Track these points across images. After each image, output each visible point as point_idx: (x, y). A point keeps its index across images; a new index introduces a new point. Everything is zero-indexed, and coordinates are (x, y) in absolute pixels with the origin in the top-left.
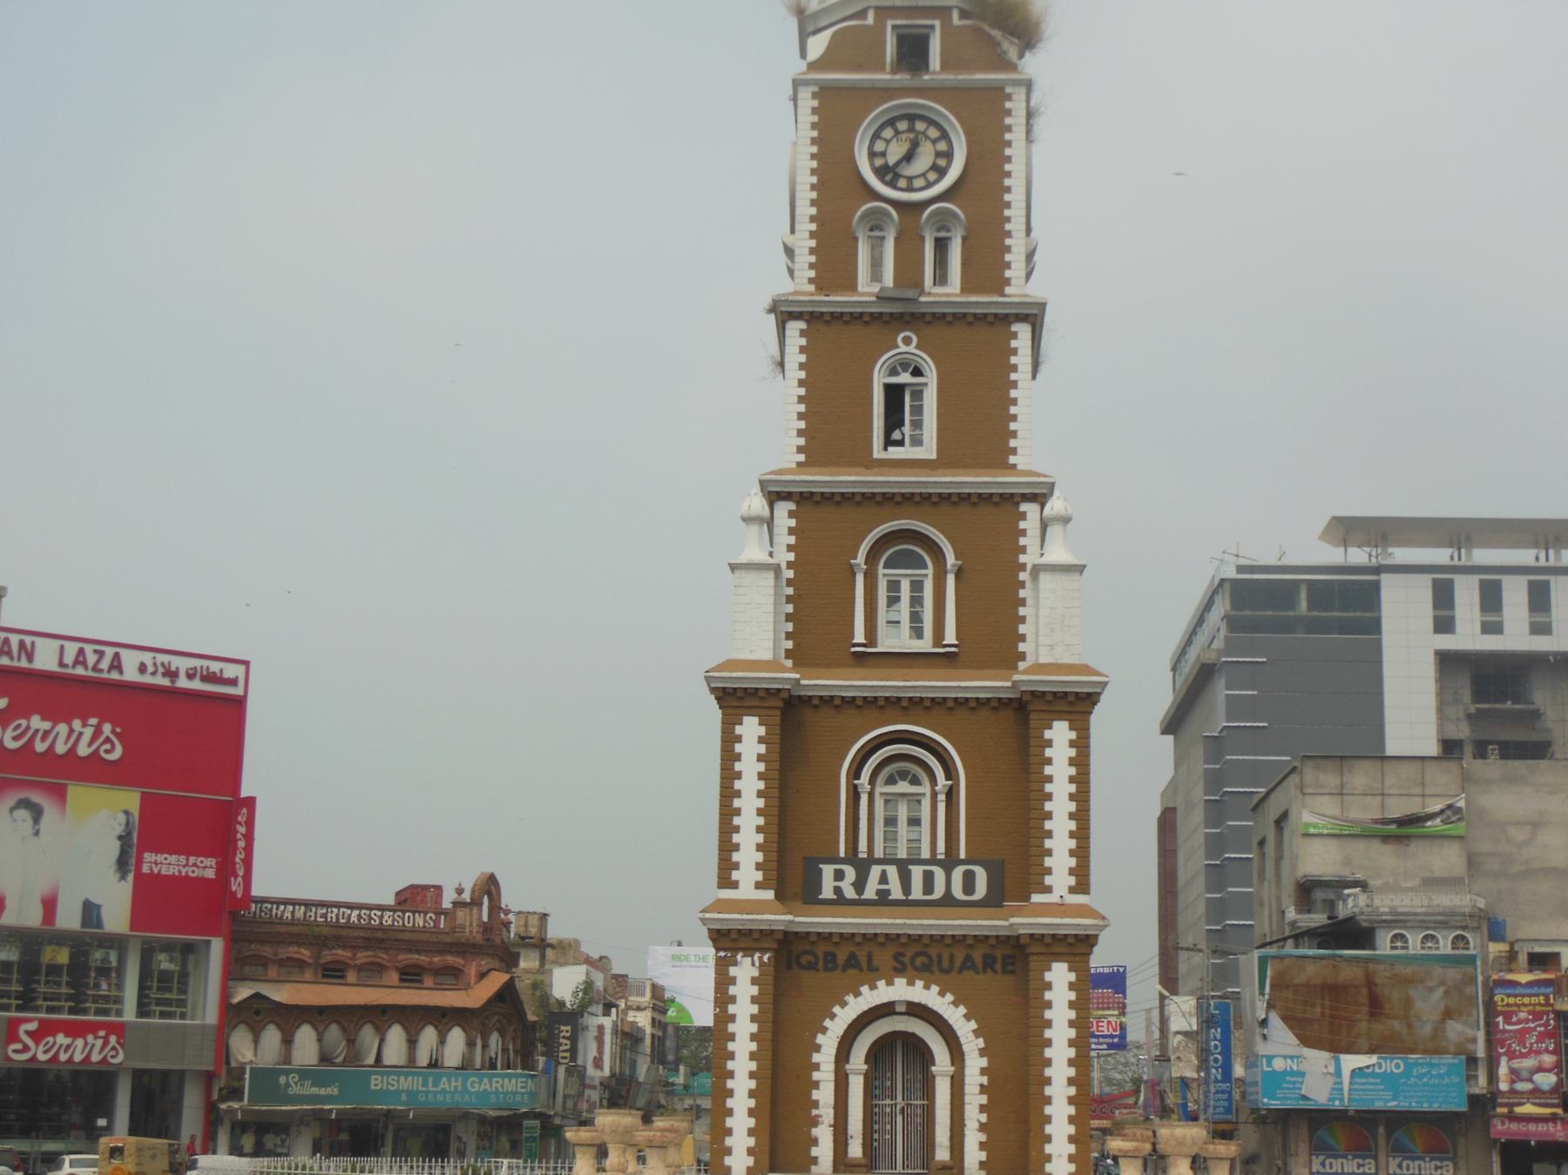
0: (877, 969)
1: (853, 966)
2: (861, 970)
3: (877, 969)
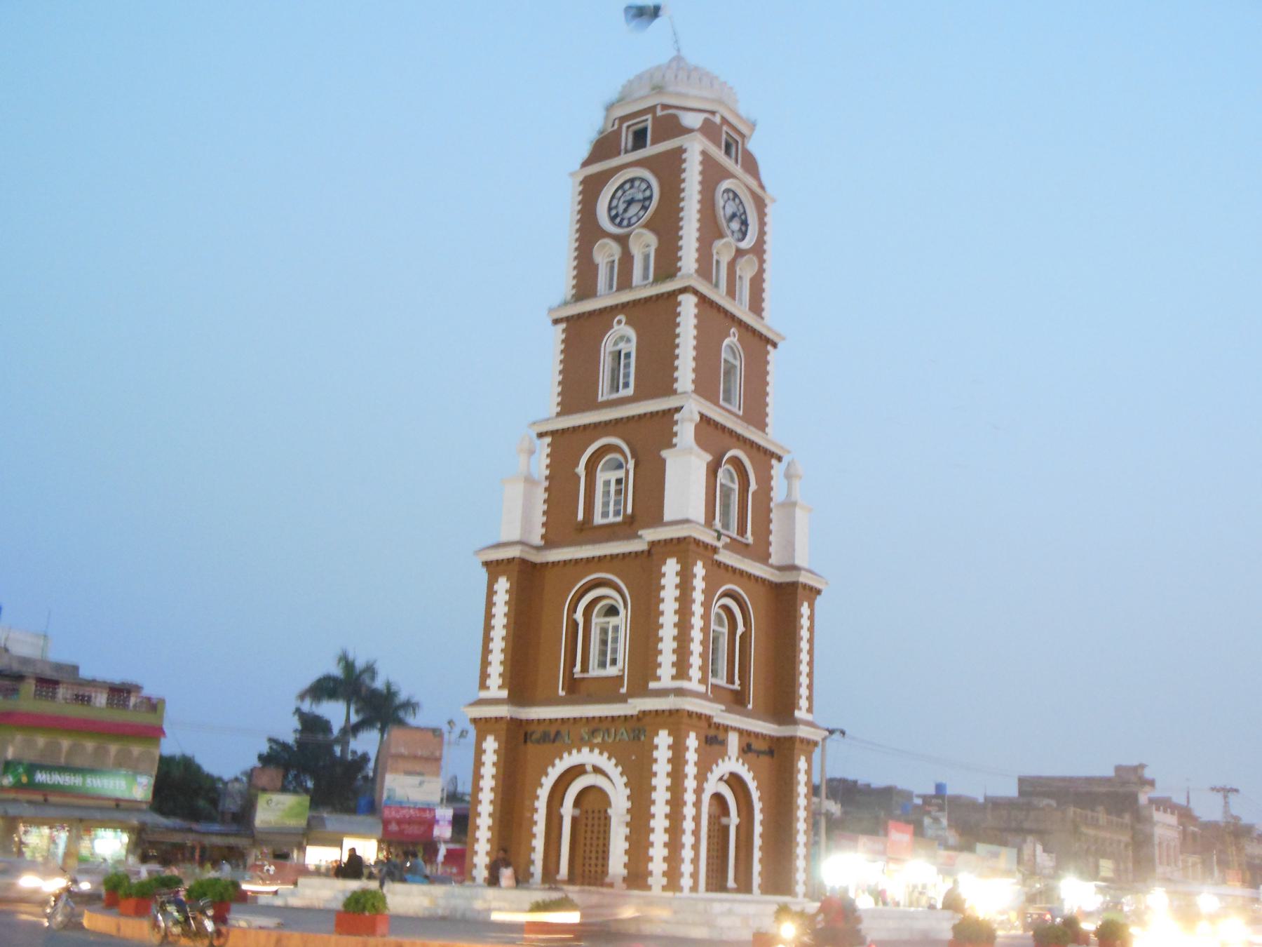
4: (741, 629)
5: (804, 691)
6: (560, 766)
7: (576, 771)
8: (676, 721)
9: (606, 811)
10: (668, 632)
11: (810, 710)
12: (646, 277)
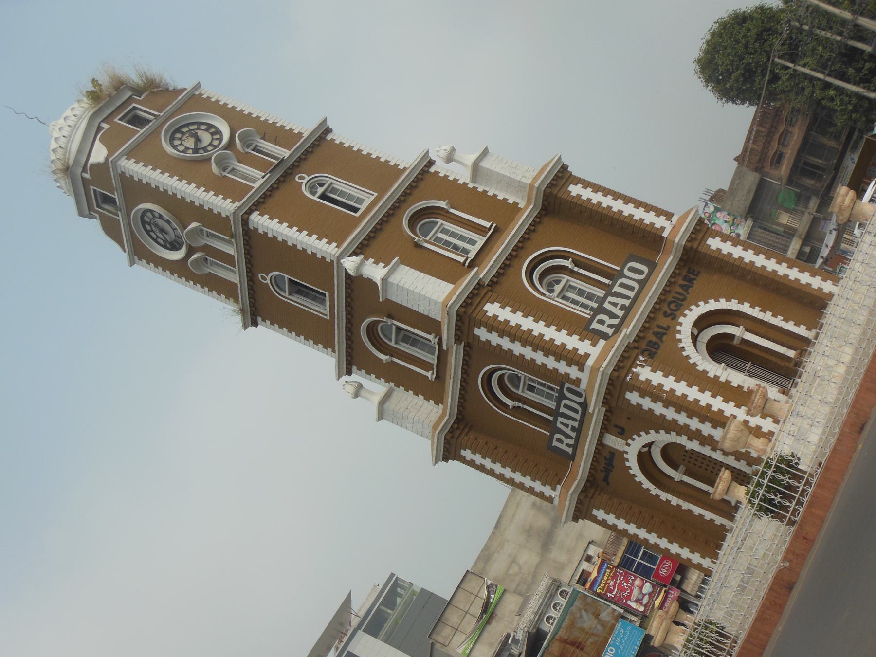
0: (669, 327)
1: (662, 337)
2: (665, 334)
3: (669, 327)
4: (568, 263)
5: (649, 218)
6: (635, 469)
7: (644, 459)
8: (618, 383)
9: (686, 451)
10: (550, 333)
11: (669, 216)
12: (229, 242)
